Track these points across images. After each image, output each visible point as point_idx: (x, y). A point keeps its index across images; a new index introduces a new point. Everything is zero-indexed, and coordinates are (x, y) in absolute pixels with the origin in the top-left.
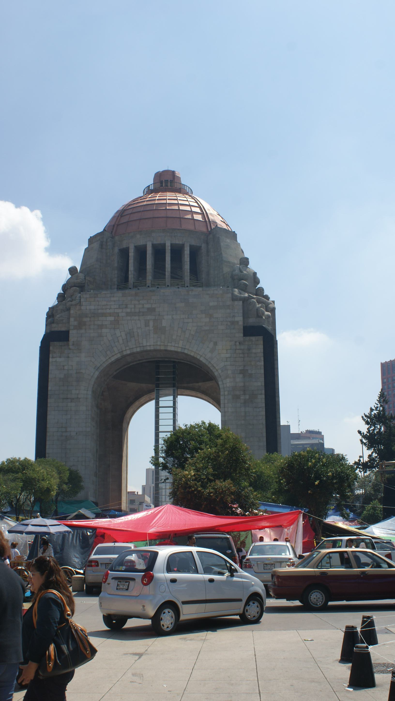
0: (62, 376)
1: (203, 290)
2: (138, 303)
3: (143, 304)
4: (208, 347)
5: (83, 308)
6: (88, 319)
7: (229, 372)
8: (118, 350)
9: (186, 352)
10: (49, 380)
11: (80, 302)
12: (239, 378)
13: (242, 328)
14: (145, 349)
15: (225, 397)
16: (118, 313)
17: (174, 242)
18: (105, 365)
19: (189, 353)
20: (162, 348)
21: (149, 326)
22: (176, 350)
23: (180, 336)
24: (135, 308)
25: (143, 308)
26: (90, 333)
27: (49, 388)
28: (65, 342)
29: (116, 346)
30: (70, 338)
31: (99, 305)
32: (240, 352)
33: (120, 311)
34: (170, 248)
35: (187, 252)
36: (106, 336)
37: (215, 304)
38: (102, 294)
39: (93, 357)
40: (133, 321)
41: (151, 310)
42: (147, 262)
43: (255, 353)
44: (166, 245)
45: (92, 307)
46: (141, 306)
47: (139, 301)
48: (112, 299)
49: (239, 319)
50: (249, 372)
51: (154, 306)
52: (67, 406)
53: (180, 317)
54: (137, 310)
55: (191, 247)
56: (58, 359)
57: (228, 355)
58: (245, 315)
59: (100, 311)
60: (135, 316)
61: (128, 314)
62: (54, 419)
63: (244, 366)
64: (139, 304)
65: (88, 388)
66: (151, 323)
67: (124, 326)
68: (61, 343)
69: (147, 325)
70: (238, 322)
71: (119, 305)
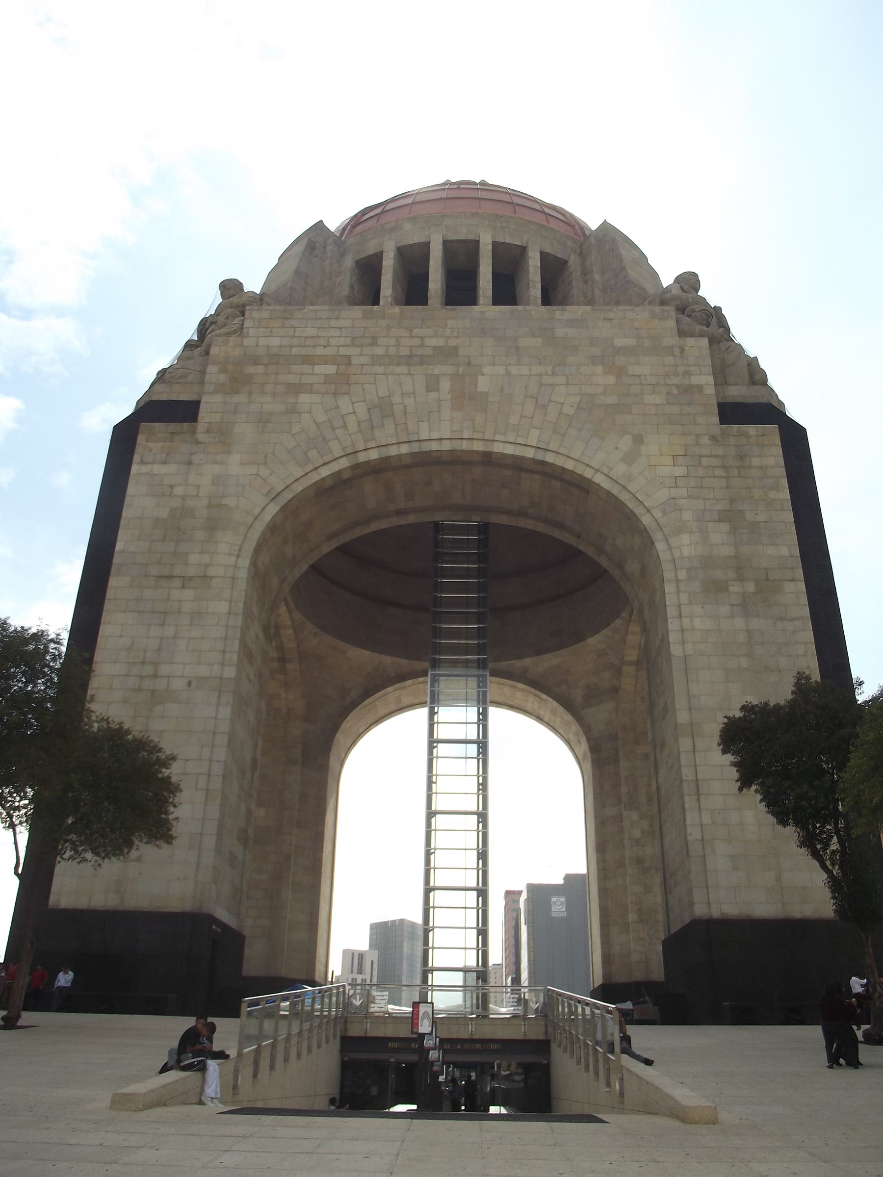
0: (164, 513)
1: (593, 310)
2: (409, 335)
3: (422, 338)
4: (617, 448)
5: (246, 342)
6: (260, 369)
7: (687, 516)
8: (343, 449)
9: (550, 458)
10: (122, 522)
11: (242, 329)
12: (719, 534)
13: (714, 402)
14: (426, 447)
15: (678, 587)
16: (348, 358)
17: (500, 239)
18: (298, 488)
19: (560, 461)
20: (478, 447)
21: (438, 390)
22: (519, 451)
23: (532, 418)
24: (398, 345)
25: (422, 346)
26: (262, 403)
27: (119, 546)
28: (185, 425)
29: (337, 438)
30: (200, 415)
31: (294, 337)
32: (715, 462)
33: (357, 351)
34: (490, 247)
35: (534, 262)
36: (310, 412)
37: (632, 342)
38: (306, 310)
39: (265, 464)
40: (390, 377)
41: (447, 353)
42: (430, 276)
43: (761, 468)
44: (481, 242)
45: (275, 341)
46: (415, 342)
47: (411, 331)
48: (334, 323)
49: (705, 380)
50: (749, 516)
51: (453, 342)
52: (168, 600)
53: (530, 370)
54: (405, 352)
55: (544, 256)
56: (157, 469)
57: (680, 471)
58: (721, 374)
59: (295, 351)
60: (398, 365)
61: (376, 360)
62: (121, 636)
63: (732, 501)
64: (411, 337)
65: (240, 550)
66: (445, 385)
67: (363, 390)
68: (173, 427)
69: (432, 385)
70: (700, 388)
71: (353, 338)
